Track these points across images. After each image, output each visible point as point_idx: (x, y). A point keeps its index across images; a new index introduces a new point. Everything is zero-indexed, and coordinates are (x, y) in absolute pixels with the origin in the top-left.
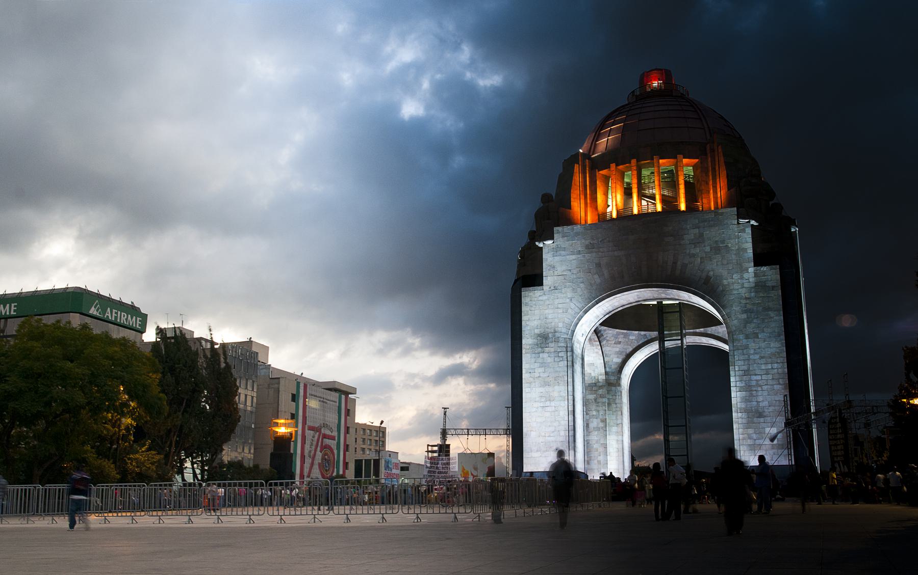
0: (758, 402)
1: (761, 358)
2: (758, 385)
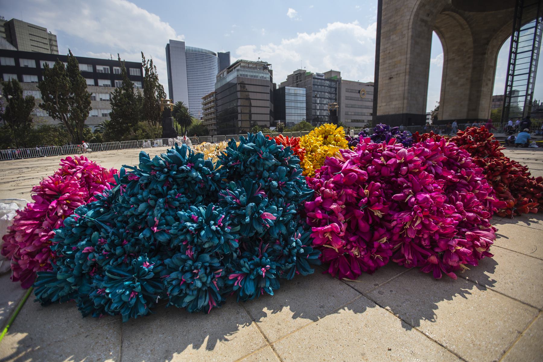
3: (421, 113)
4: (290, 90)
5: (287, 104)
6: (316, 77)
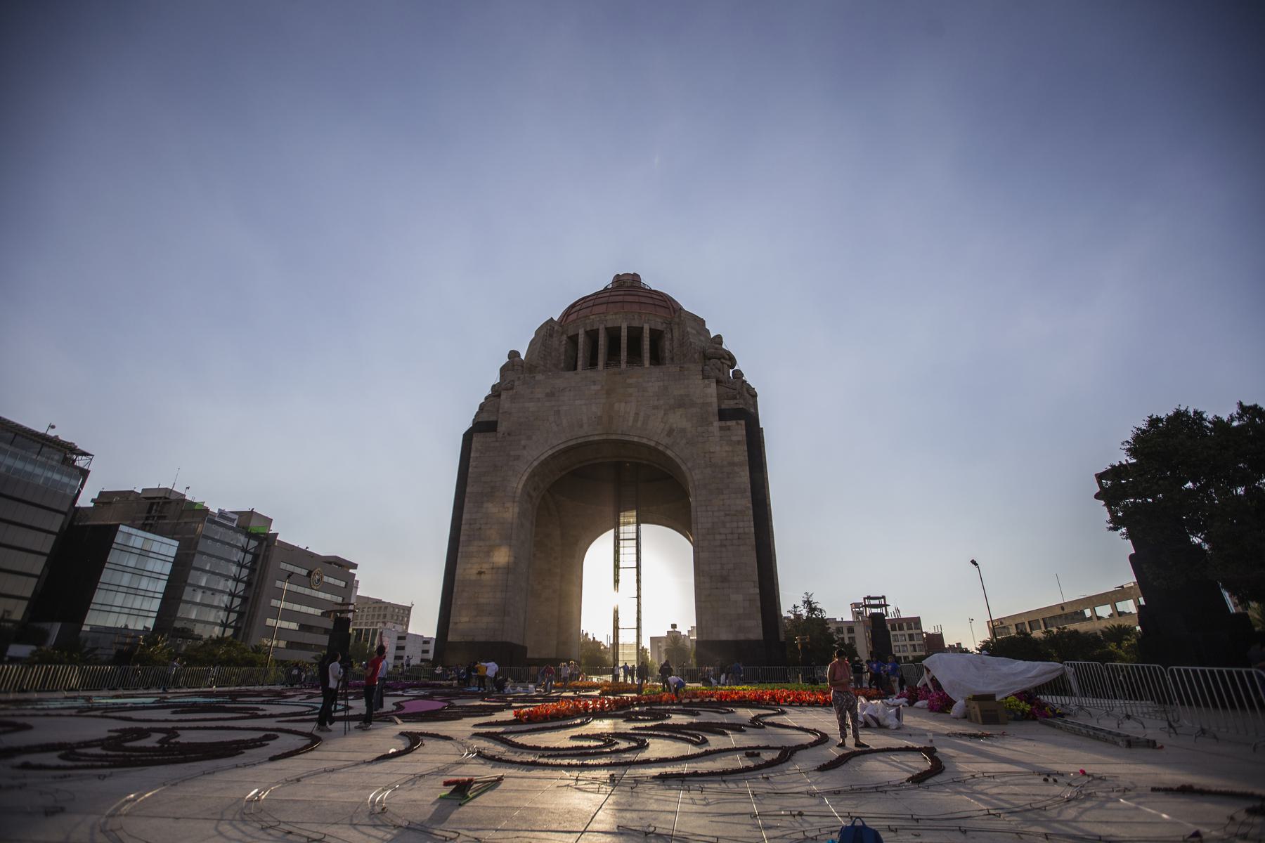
0: (721, 564)
1: (728, 515)
2: (722, 545)
3: (521, 643)
4: (132, 537)
5: (106, 576)
6: (216, 519)
